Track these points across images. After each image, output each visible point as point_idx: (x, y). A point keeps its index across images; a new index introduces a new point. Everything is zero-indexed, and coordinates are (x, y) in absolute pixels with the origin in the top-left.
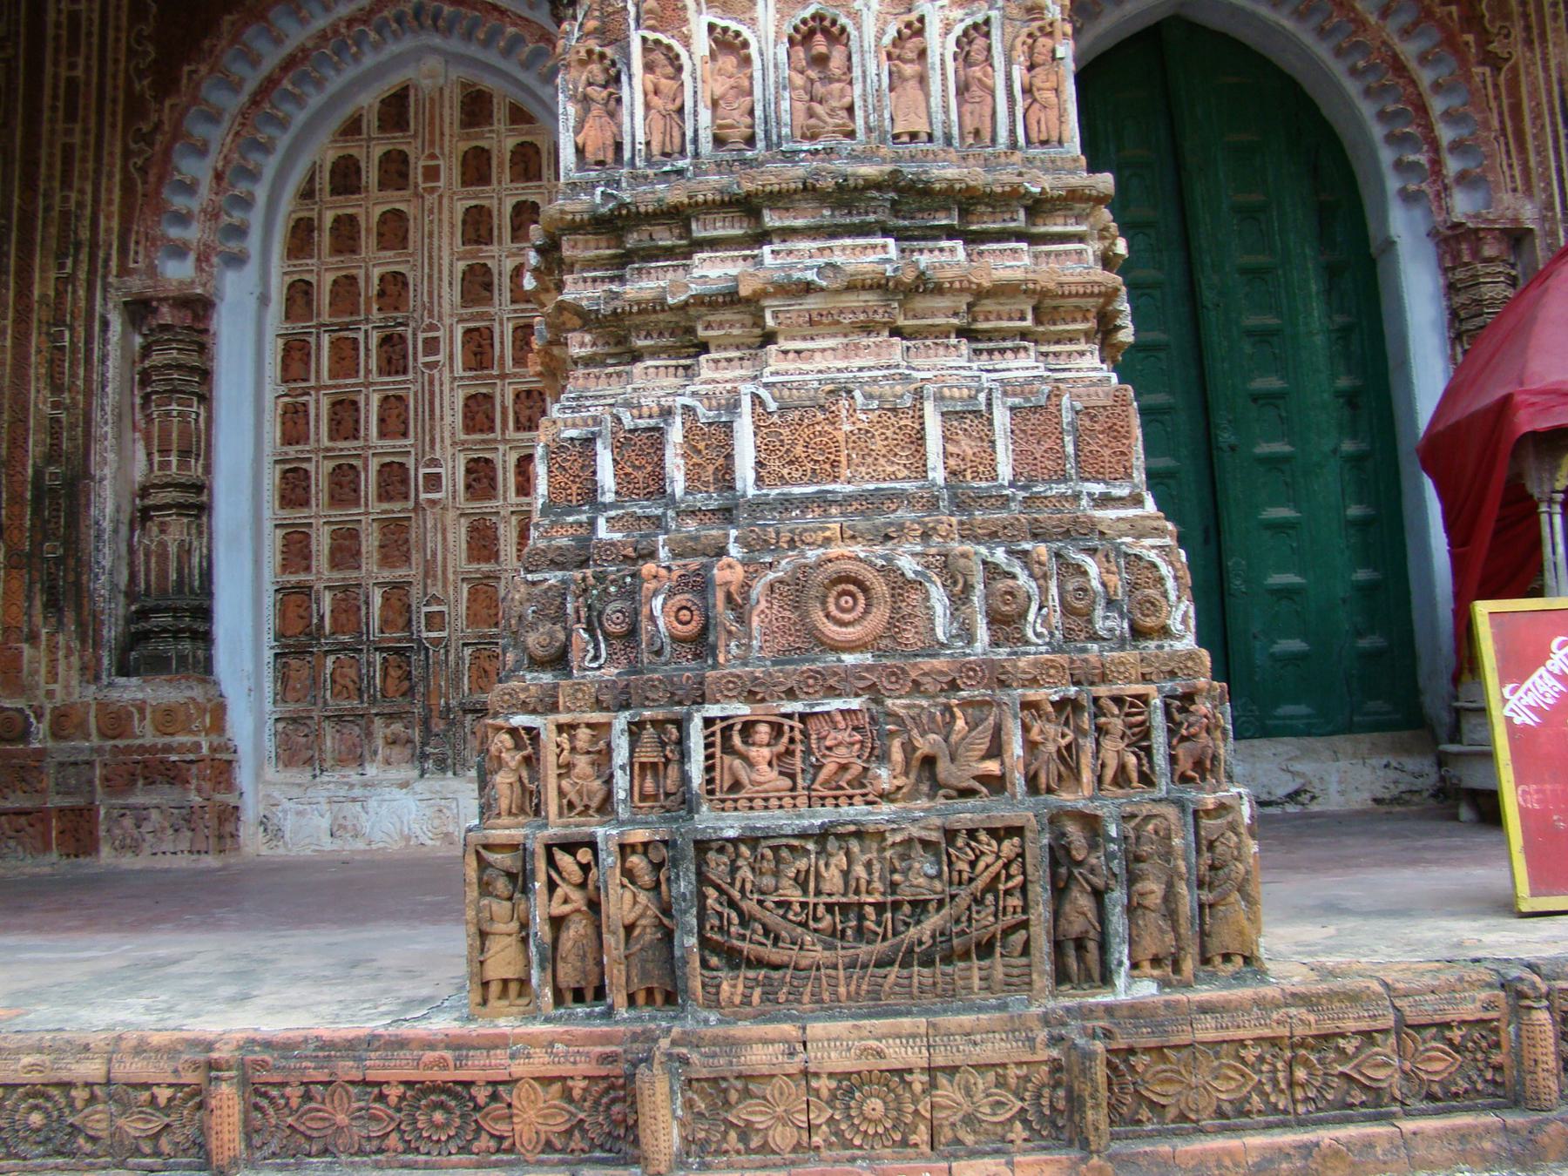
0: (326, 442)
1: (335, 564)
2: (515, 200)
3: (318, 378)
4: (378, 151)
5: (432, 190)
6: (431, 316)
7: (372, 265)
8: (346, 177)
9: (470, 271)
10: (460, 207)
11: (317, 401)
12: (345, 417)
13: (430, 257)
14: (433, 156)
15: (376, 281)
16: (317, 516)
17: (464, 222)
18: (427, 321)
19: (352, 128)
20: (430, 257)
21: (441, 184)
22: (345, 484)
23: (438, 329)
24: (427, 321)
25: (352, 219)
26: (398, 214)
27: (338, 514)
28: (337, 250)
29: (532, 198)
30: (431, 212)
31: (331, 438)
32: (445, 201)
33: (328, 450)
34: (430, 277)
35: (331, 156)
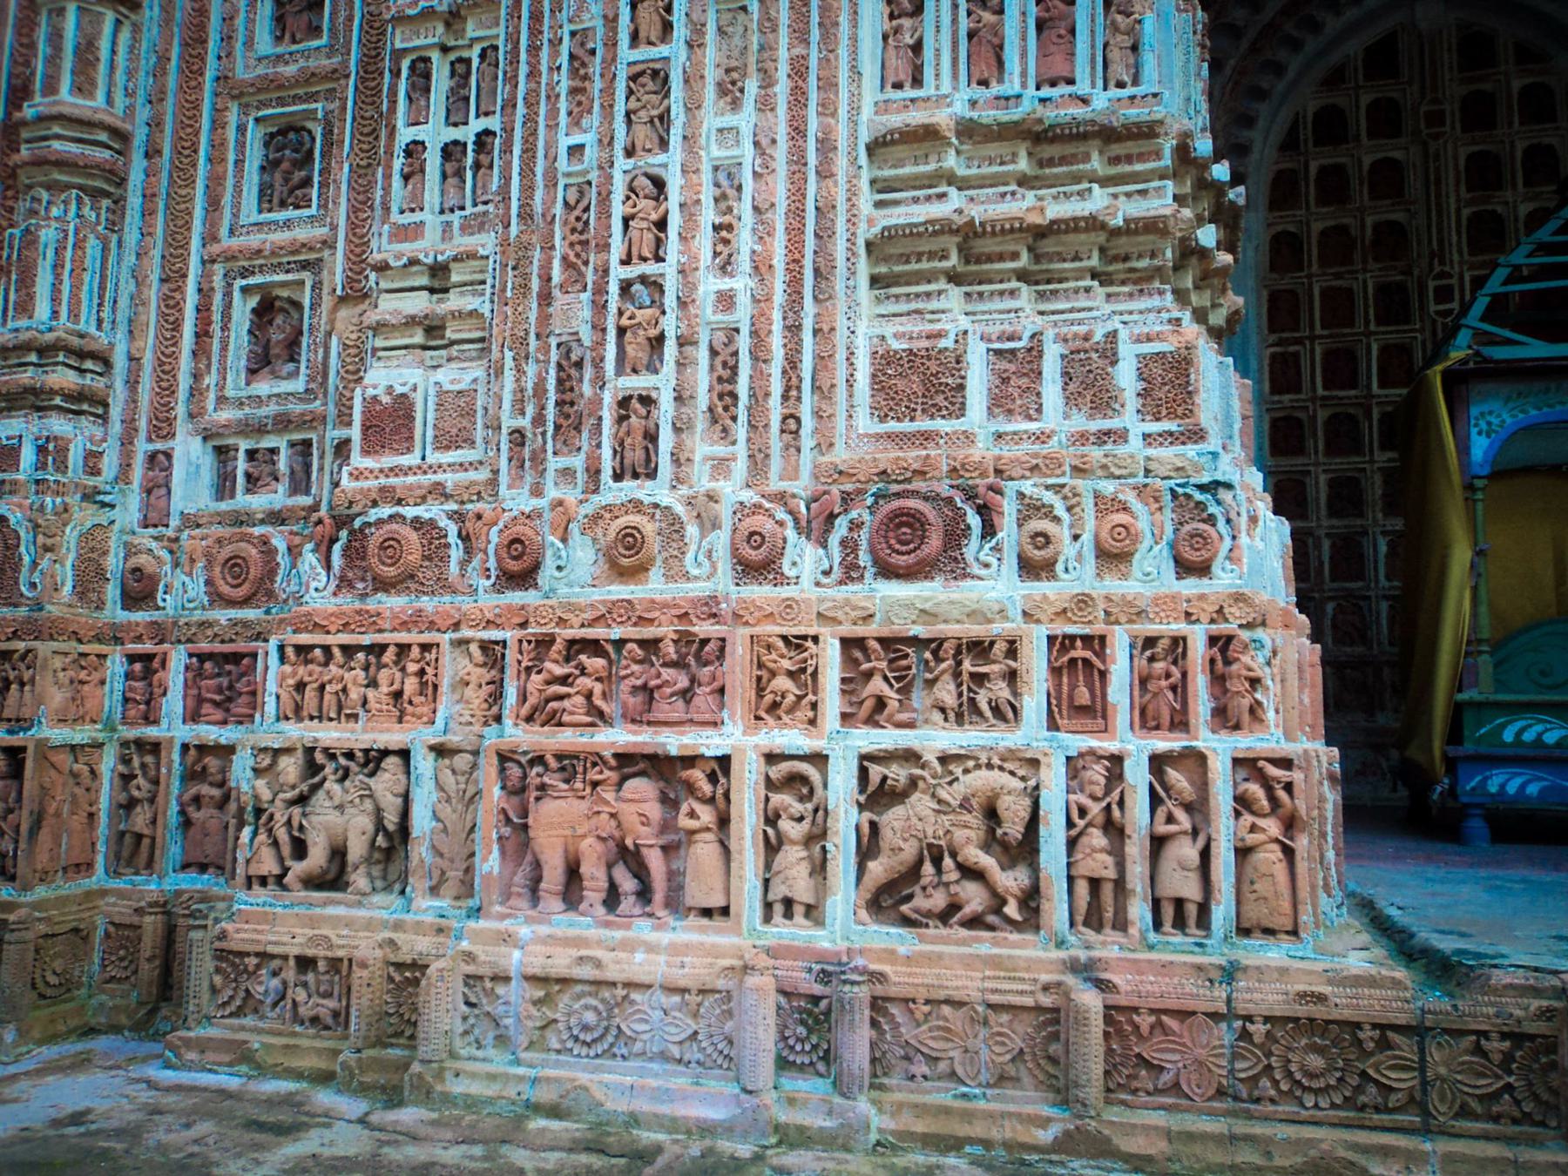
0: (1320, 391)
1: (1333, 512)
2: (1527, 143)
3: (1312, 327)
4: (1365, 99)
5: (1436, 137)
6: (1442, 263)
7: (1367, 215)
8: (1331, 127)
9: (1475, 219)
10: (1463, 153)
11: (1312, 351)
12: (1341, 367)
13: (1438, 204)
14: (1435, 101)
15: (1369, 232)
16: (1317, 464)
17: (1467, 169)
18: (1437, 269)
19: (1334, 79)
20: (1438, 204)
21: (1448, 128)
22: (1344, 434)
23: (1450, 276)
24: (1437, 269)
25: (1339, 170)
26: (1393, 163)
27: (1339, 463)
28: (1323, 200)
29: (1546, 141)
30: (1437, 157)
31: (1325, 388)
32: (1450, 147)
33: (1324, 398)
34: (1440, 223)
35: (1312, 108)
